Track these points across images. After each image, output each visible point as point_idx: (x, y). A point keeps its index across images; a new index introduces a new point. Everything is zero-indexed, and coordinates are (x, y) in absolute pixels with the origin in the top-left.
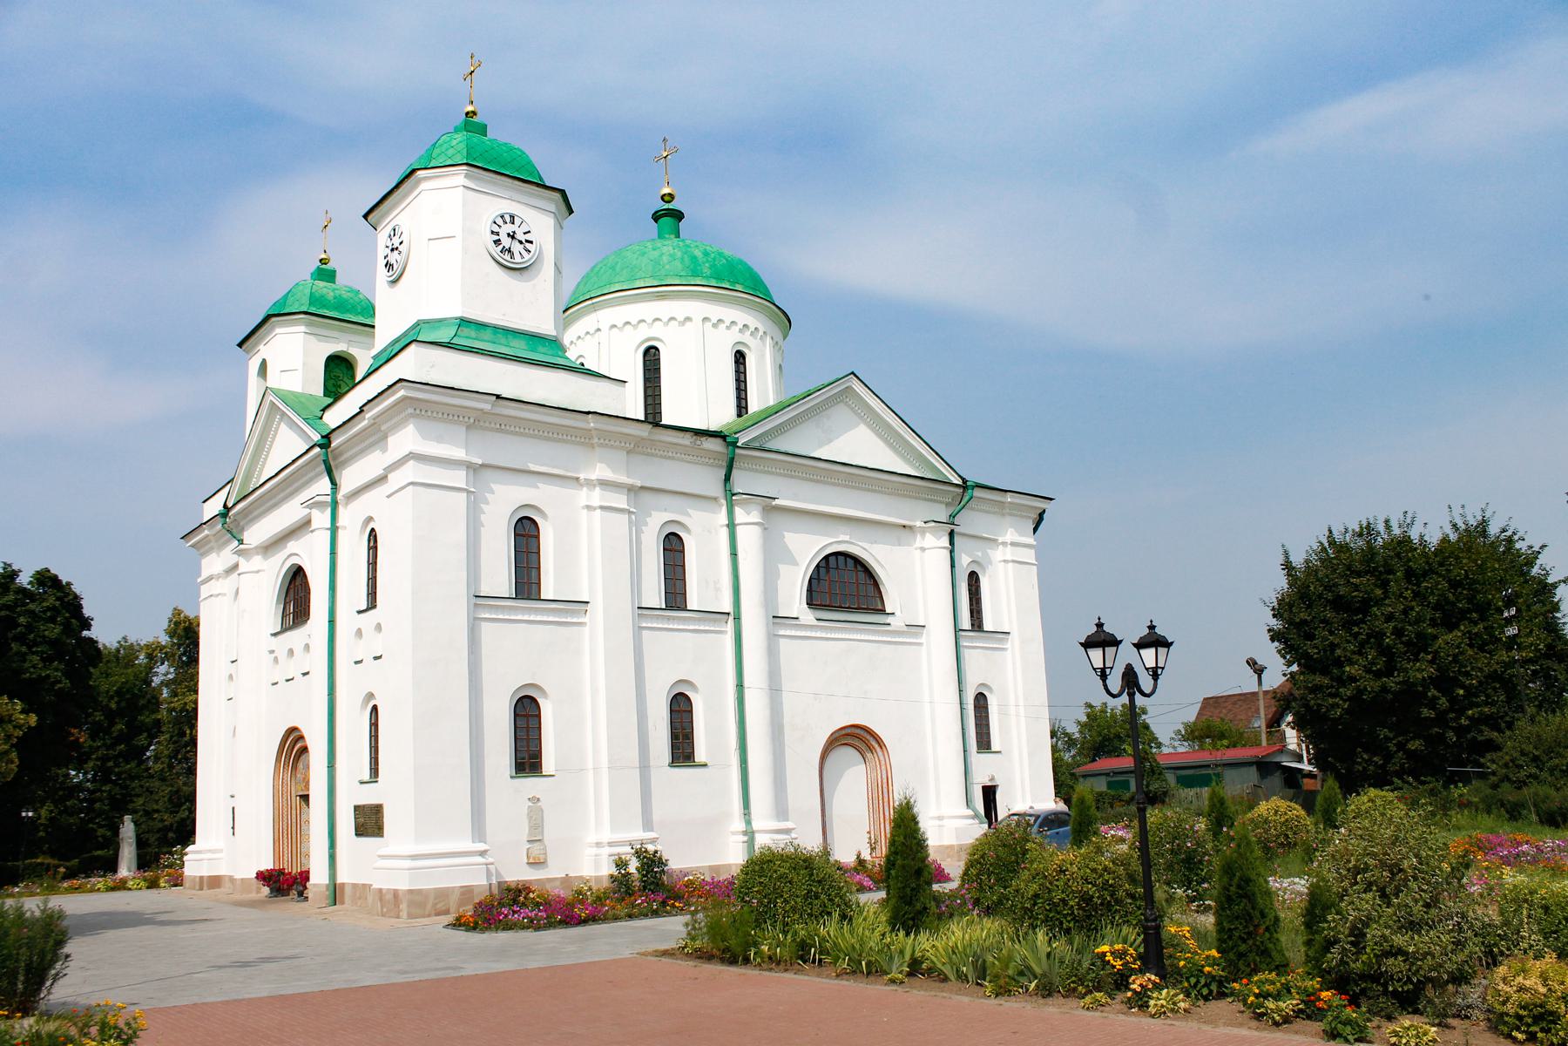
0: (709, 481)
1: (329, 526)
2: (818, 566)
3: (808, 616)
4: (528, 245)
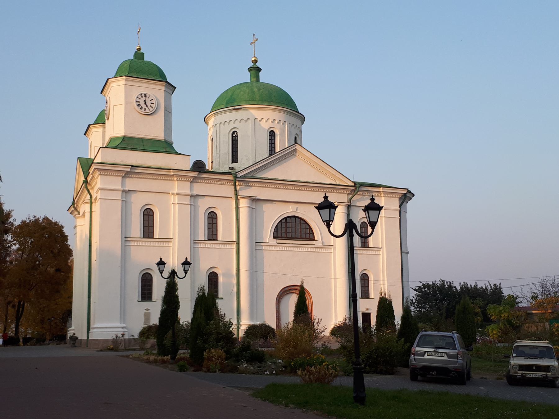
0: (228, 190)
1: (89, 211)
3: (274, 242)
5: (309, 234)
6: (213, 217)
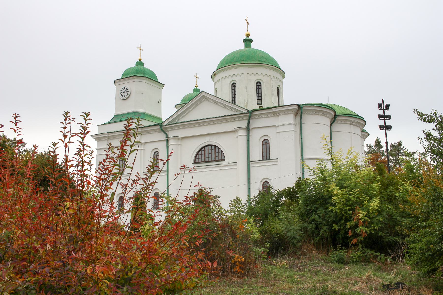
0: (162, 136)
2: (200, 150)
4: (128, 93)
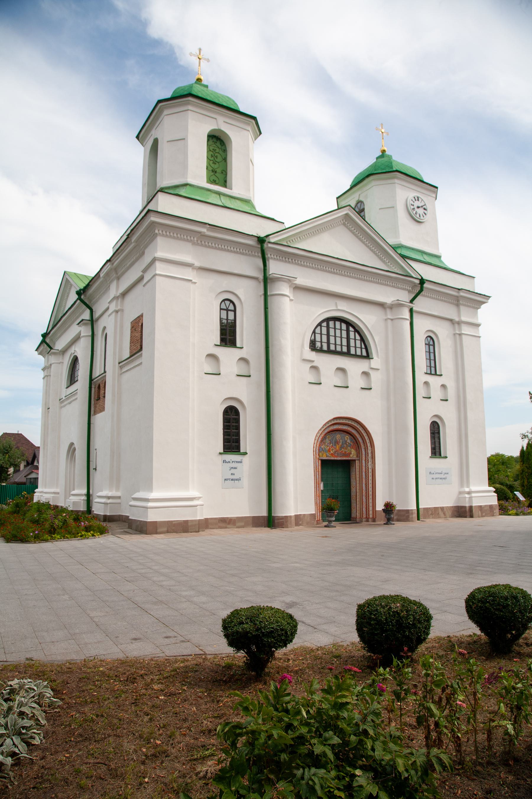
5: (361, 348)
6: (229, 308)
